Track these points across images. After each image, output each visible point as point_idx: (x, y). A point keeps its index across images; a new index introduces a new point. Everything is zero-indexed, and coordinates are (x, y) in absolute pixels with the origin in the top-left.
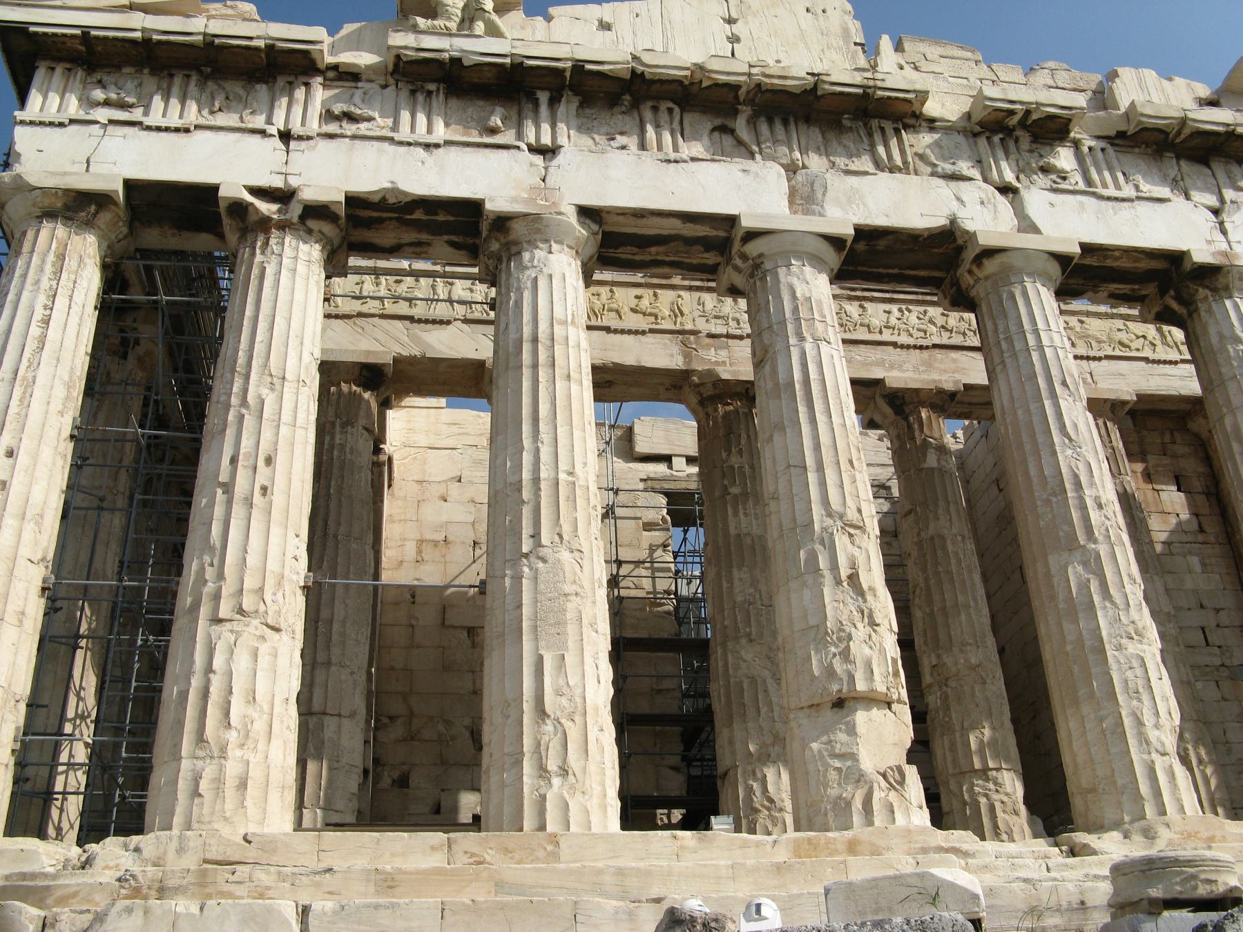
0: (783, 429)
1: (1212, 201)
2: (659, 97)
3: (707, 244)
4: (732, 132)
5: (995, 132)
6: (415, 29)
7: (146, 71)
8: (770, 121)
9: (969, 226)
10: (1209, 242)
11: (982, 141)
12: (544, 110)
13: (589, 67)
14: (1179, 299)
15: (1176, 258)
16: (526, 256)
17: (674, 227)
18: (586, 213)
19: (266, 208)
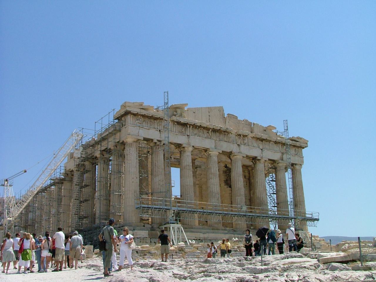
0: (212, 179)
1: (261, 147)
2: (201, 128)
3: (203, 149)
4: (209, 133)
5: (239, 135)
6: (175, 116)
7: (142, 117)
8: (213, 132)
9: (234, 151)
10: (260, 155)
11: (237, 137)
12: (188, 128)
13: (196, 124)
14: (255, 161)
15: (256, 157)
16: (186, 152)
17: (202, 148)
18: (193, 146)
19: (158, 143)
